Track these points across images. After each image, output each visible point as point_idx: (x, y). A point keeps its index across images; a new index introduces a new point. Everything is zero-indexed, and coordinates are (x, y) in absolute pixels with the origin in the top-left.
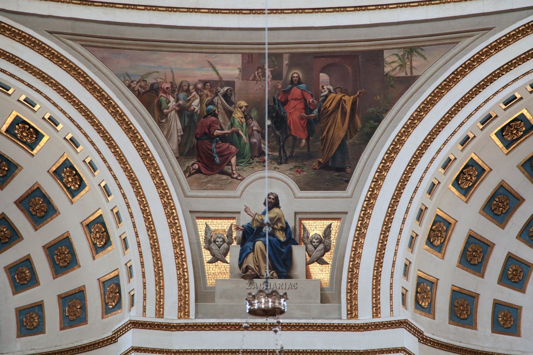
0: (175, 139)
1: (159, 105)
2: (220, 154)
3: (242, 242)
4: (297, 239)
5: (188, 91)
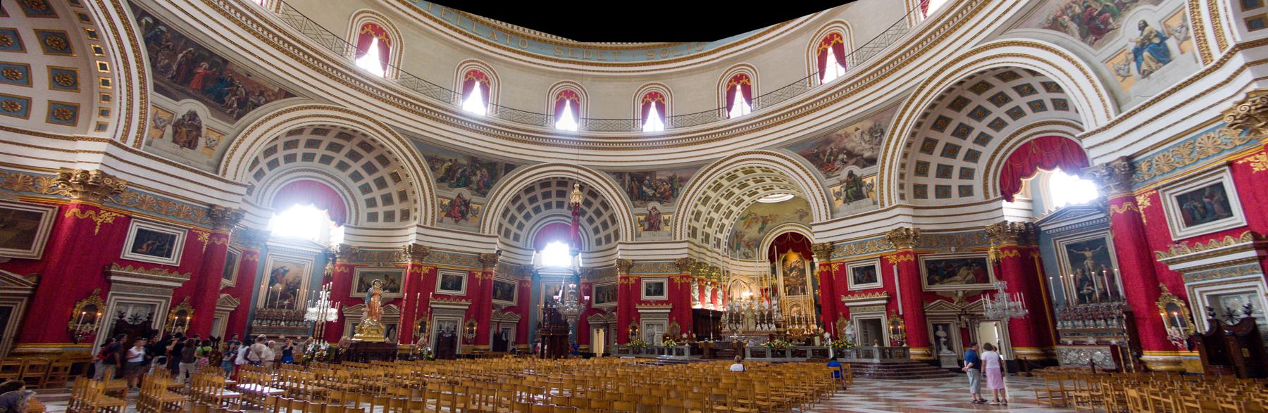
0: (1077, 33)
1: (1062, 25)
2: (1102, 23)
3: (1136, 59)
4: (1167, 35)
5: (1071, 7)
